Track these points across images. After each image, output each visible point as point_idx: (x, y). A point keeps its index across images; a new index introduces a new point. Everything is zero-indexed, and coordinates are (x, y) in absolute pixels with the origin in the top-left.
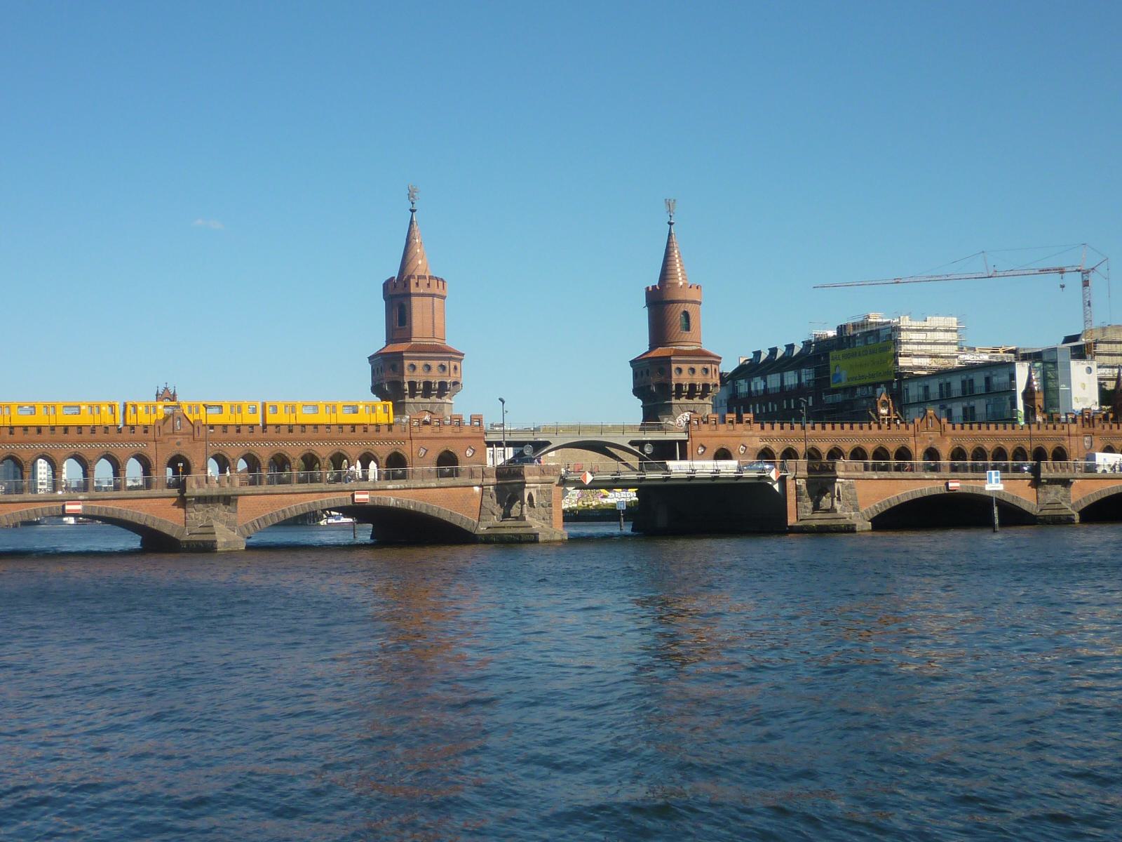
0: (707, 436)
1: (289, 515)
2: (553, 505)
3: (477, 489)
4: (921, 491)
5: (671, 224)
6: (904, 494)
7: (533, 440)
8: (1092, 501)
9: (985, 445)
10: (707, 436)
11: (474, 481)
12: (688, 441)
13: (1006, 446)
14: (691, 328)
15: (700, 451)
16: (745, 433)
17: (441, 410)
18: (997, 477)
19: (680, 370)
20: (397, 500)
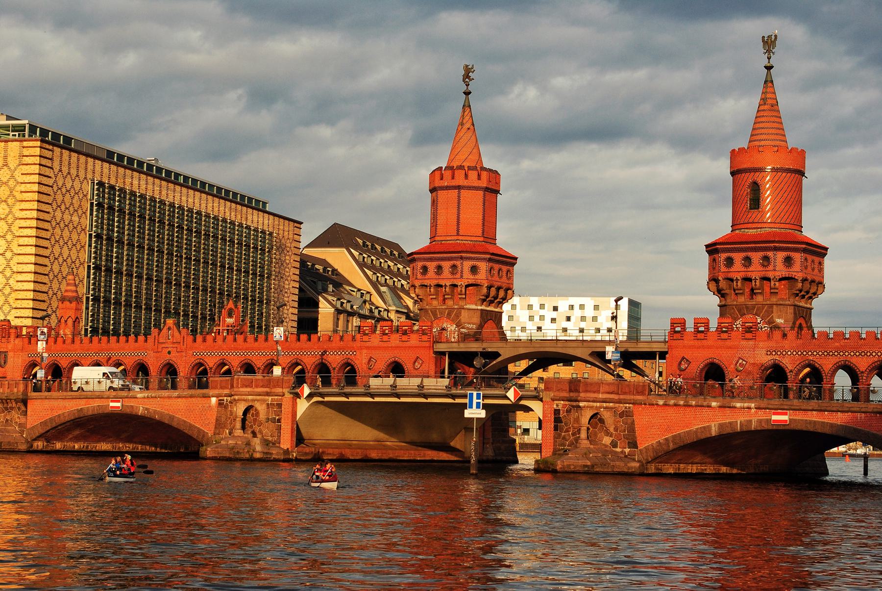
0: (691, 347)
1: (63, 420)
2: (282, 421)
3: (214, 400)
4: (730, 423)
5: (769, 68)
6: (704, 428)
7: (481, 350)
10: (691, 347)
11: (211, 392)
12: (666, 353)
15: (683, 367)
16: (744, 343)
17: (458, 315)
18: (478, 401)
19: (730, 262)
20: (147, 409)
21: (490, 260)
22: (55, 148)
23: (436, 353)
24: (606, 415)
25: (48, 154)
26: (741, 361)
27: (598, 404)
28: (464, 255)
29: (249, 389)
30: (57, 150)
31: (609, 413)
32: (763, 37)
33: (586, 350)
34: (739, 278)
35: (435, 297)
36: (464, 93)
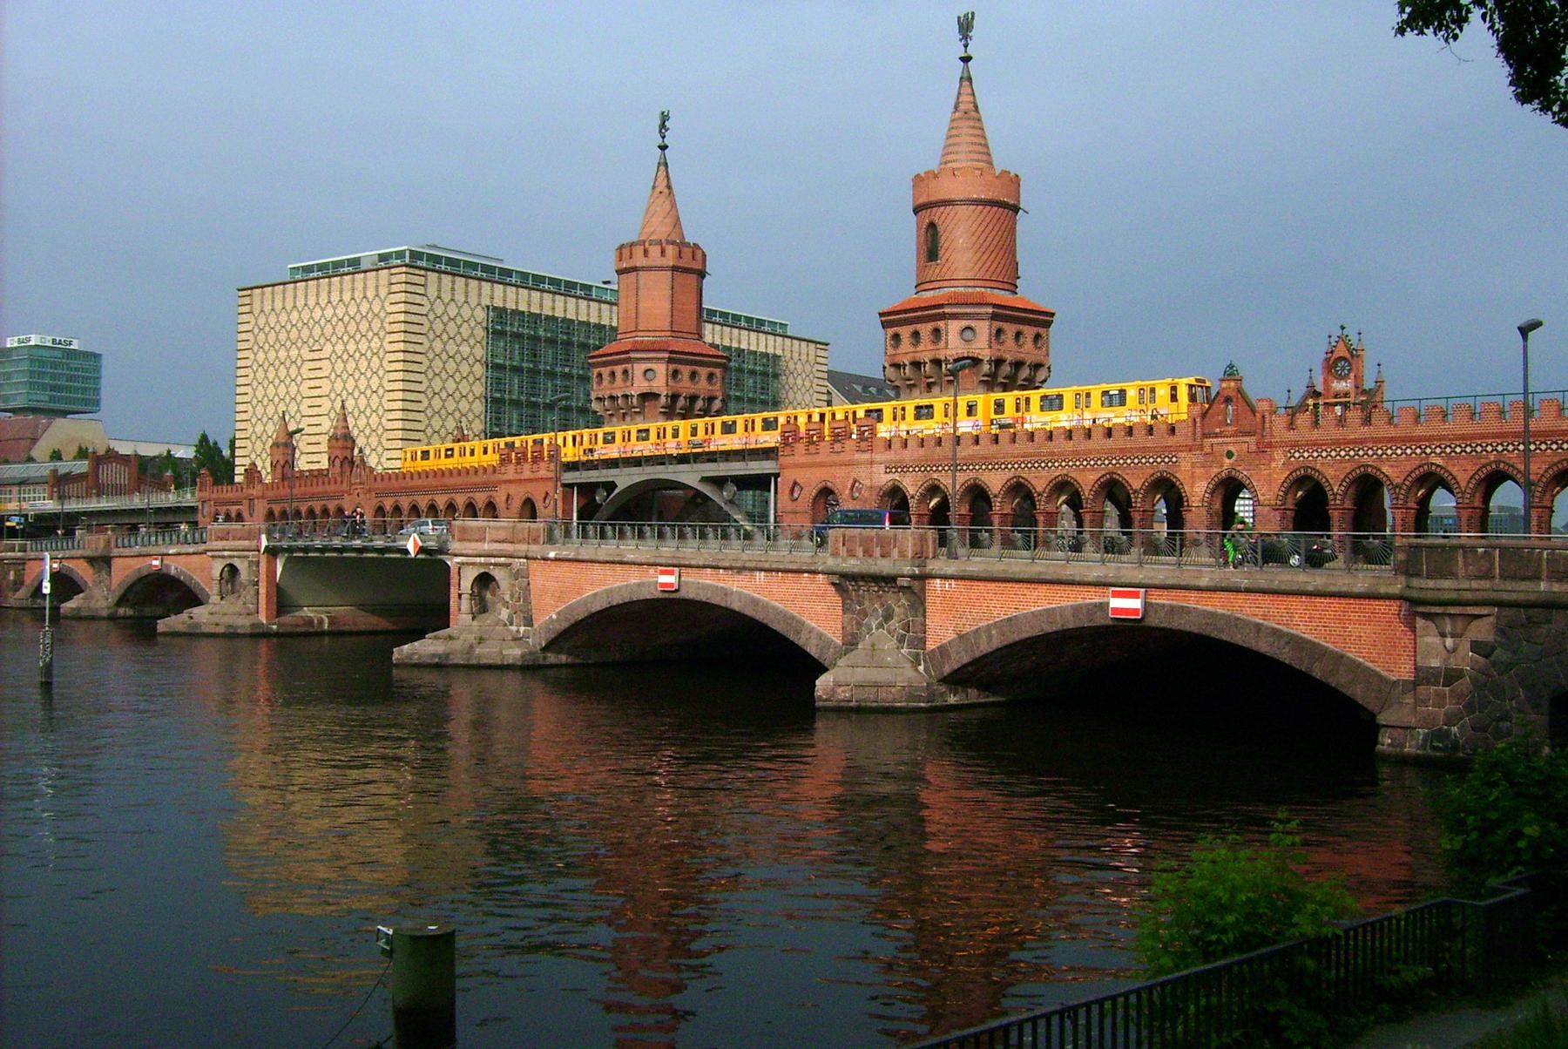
8: (985, 647)
9: (1385, 469)
13: (1454, 471)
14: (941, 253)
16: (858, 456)
21: (670, 361)
22: (429, 273)
23: (564, 485)
24: (498, 574)
25: (421, 280)
26: (857, 484)
27: (483, 560)
28: (632, 355)
29: (224, 543)
30: (433, 276)
31: (502, 572)
32: (959, 18)
33: (696, 474)
34: (907, 363)
35: (638, 410)
36: (659, 147)
